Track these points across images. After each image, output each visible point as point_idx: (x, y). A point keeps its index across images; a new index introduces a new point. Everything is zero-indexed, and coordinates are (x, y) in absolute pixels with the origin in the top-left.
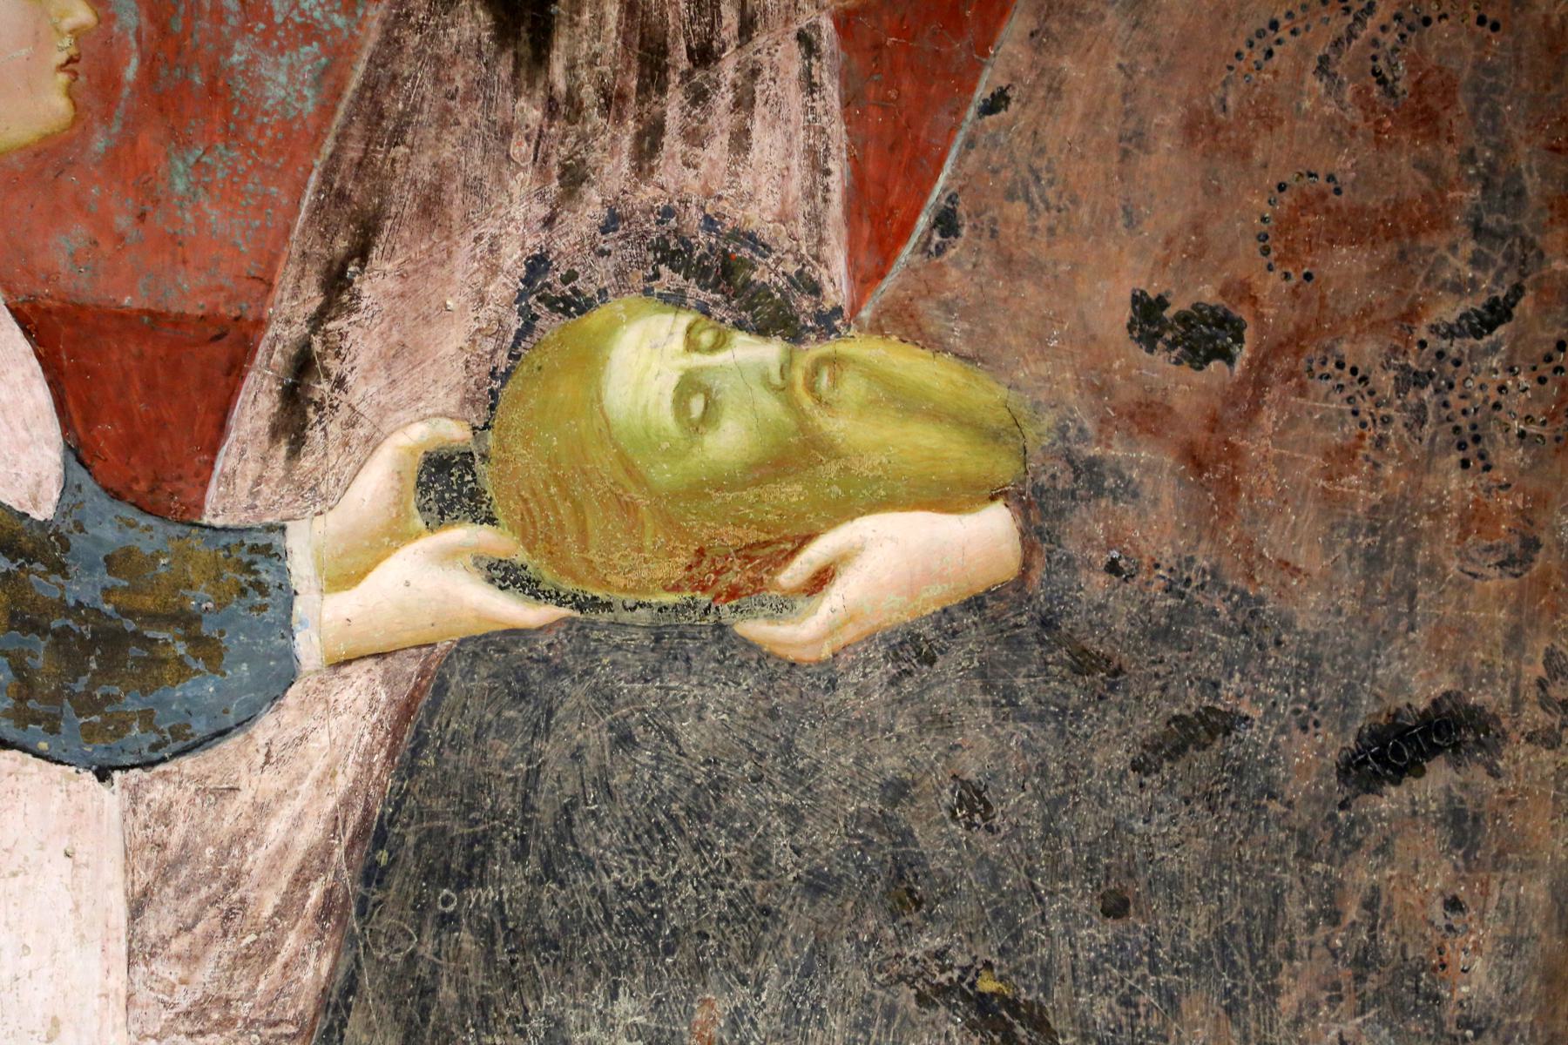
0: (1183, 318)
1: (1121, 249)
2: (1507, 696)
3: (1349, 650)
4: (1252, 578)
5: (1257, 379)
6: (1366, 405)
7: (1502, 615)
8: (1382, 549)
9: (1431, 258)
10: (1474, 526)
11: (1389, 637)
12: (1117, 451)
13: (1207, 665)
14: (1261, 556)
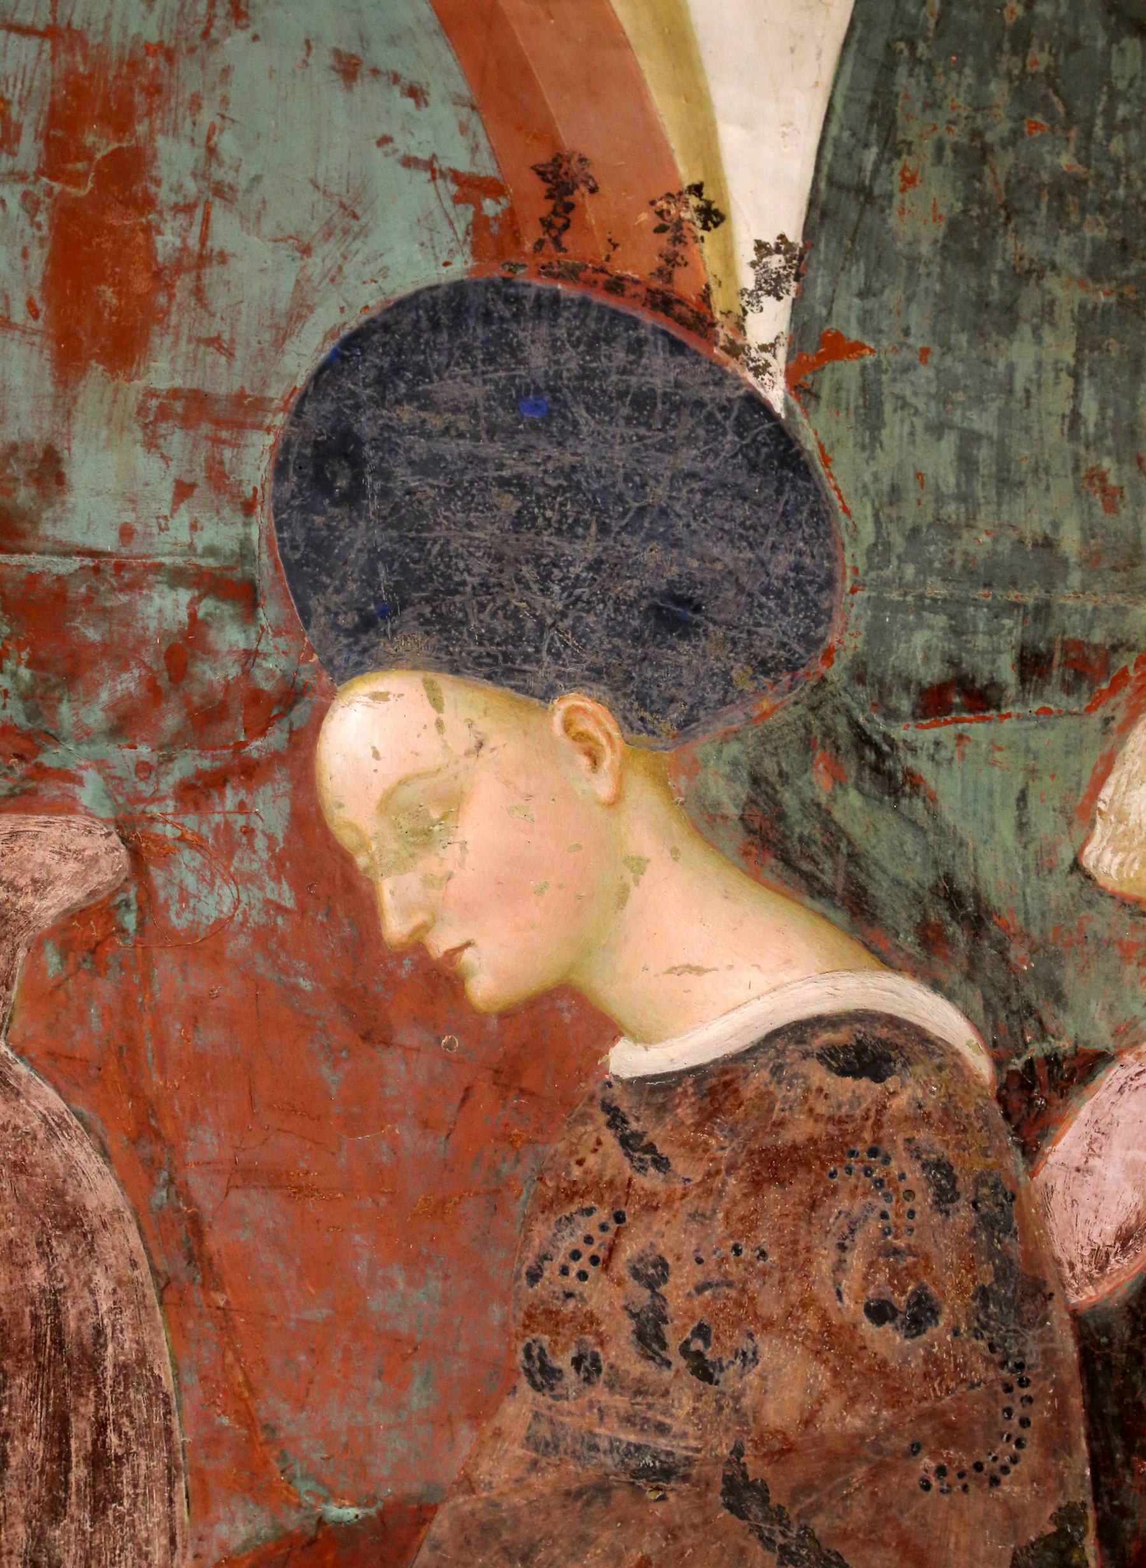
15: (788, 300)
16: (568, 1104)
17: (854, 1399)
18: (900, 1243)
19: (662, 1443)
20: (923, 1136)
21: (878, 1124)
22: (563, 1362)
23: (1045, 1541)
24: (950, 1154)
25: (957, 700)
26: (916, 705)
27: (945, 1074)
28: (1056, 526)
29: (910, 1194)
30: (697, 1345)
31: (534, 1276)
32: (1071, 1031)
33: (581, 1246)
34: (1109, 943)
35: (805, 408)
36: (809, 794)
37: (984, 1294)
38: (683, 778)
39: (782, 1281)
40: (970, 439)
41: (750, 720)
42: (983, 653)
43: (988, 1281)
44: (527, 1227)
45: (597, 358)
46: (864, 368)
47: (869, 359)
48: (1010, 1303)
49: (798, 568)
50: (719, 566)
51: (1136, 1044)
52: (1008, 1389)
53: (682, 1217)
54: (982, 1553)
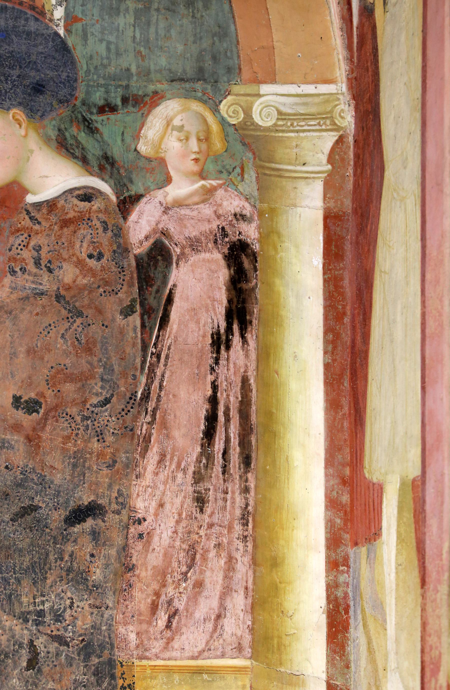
0: (26, 402)
1: (10, 383)
2: (108, 501)
3: (68, 489)
4: (43, 470)
5: (45, 418)
6: (73, 425)
7: (107, 480)
8: (77, 462)
9: (90, 387)
10: (100, 457)
11: (78, 486)
12: (8, 437)
13: (31, 493)
14: (46, 464)
15: (64, 7)
16: (17, 210)
17: (85, 276)
18: (95, 240)
19: (41, 287)
20: (100, 215)
21: (90, 213)
22: (17, 269)
23: (128, 306)
24: (106, 219)
25: (107, 109)
26: (97, 111)
27: (105, 200)
28: (130, 65)
29: (97, 229)
30: (49, 265)
31: (10, 250)
32: (134, 190)
33: (21, 243)
34: (143, 168)
35: (69, 35)
36: (72, 133)
37: (114, 251)
38: (42, 130)
39: (68, 250)
40: (109, 43)
41: (58, 115)
42: (113, 97)
43: (115, 248)
44: (8, 239)
45: (17, 23)
46: (83, 25)
47: (84, 22)
48: (120, 253)
49: (68, 76)
50: (49, 76)
51: (149, 192)
52: (120, 273)
53: (44, 235)
54: (114, 309)
